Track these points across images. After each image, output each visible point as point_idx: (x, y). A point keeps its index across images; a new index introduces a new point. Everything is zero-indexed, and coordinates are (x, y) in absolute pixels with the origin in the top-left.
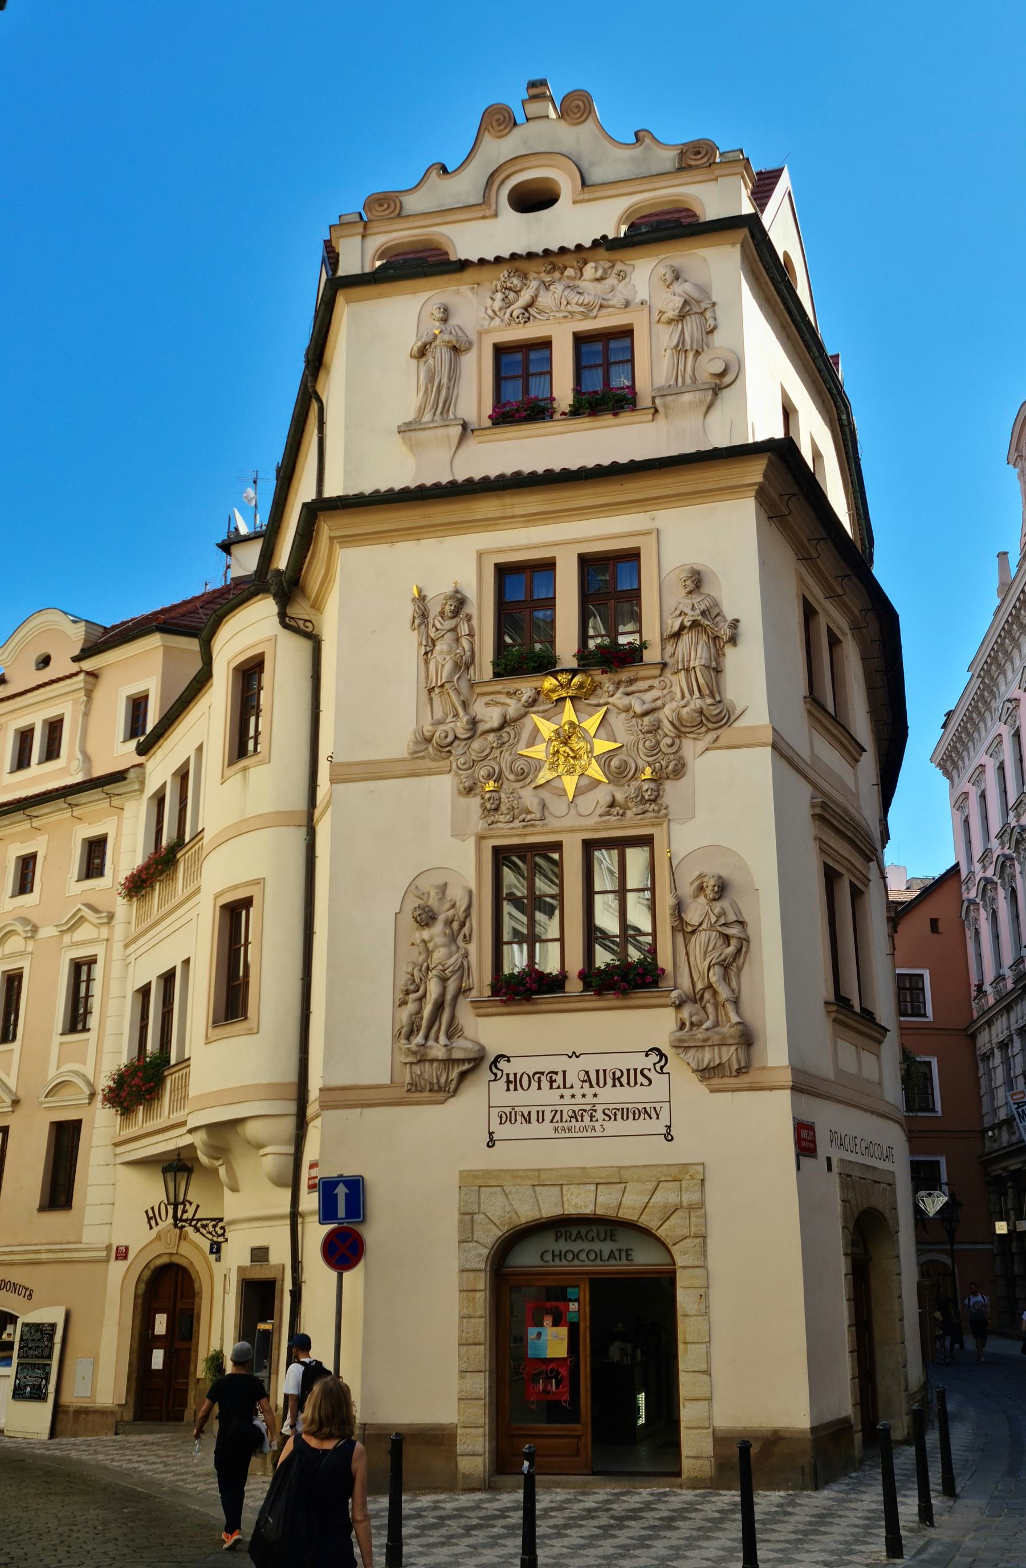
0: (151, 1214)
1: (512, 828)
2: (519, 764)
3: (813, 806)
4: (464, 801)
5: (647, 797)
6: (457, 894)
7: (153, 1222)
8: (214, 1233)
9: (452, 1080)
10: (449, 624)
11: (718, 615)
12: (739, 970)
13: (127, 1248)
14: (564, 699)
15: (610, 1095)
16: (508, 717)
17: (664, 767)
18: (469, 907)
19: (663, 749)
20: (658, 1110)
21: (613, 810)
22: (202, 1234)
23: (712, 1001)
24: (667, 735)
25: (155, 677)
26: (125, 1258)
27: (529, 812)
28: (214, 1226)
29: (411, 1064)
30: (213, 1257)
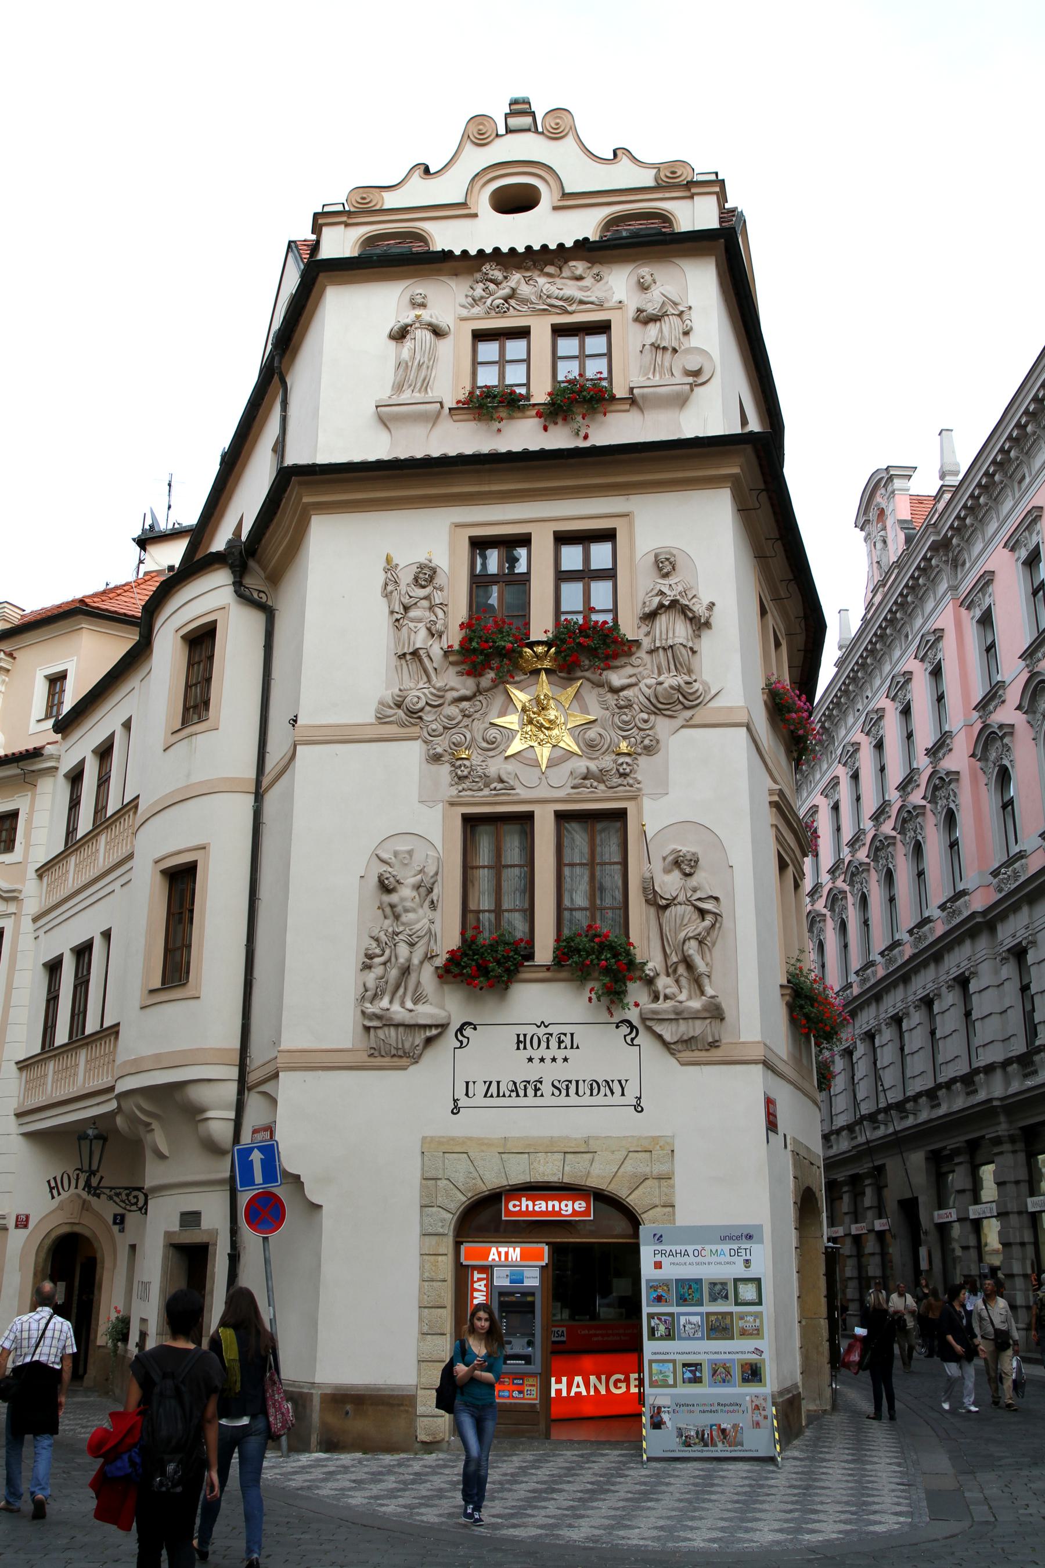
0: (53, 1184)
1: (483, 797)
2: (493, 733)
3: (771, 792)
4: (434, 768)
5: (621, 771)
6: (425, 858)
7: (55, 1192)
8: (127, 1202)
9: (417, 1046)
10: (422, 593)
11: (694, 596)
12: (714, 944)
13: (27, 1217)
14: (540, 670)
16: (481, 686)
17: (639, 741)
18: (437, 874)
19: (640, 725)
20: (623, 1083)
21: (586, 782)
22: (115, 1202)
23: (685, 974)
24: (642, 711)
25: (75, 658)
26: (26, 1226)
27: (502, 781)
28: (128, 1195)
29: (376, 1028)
30: (116, 1228)
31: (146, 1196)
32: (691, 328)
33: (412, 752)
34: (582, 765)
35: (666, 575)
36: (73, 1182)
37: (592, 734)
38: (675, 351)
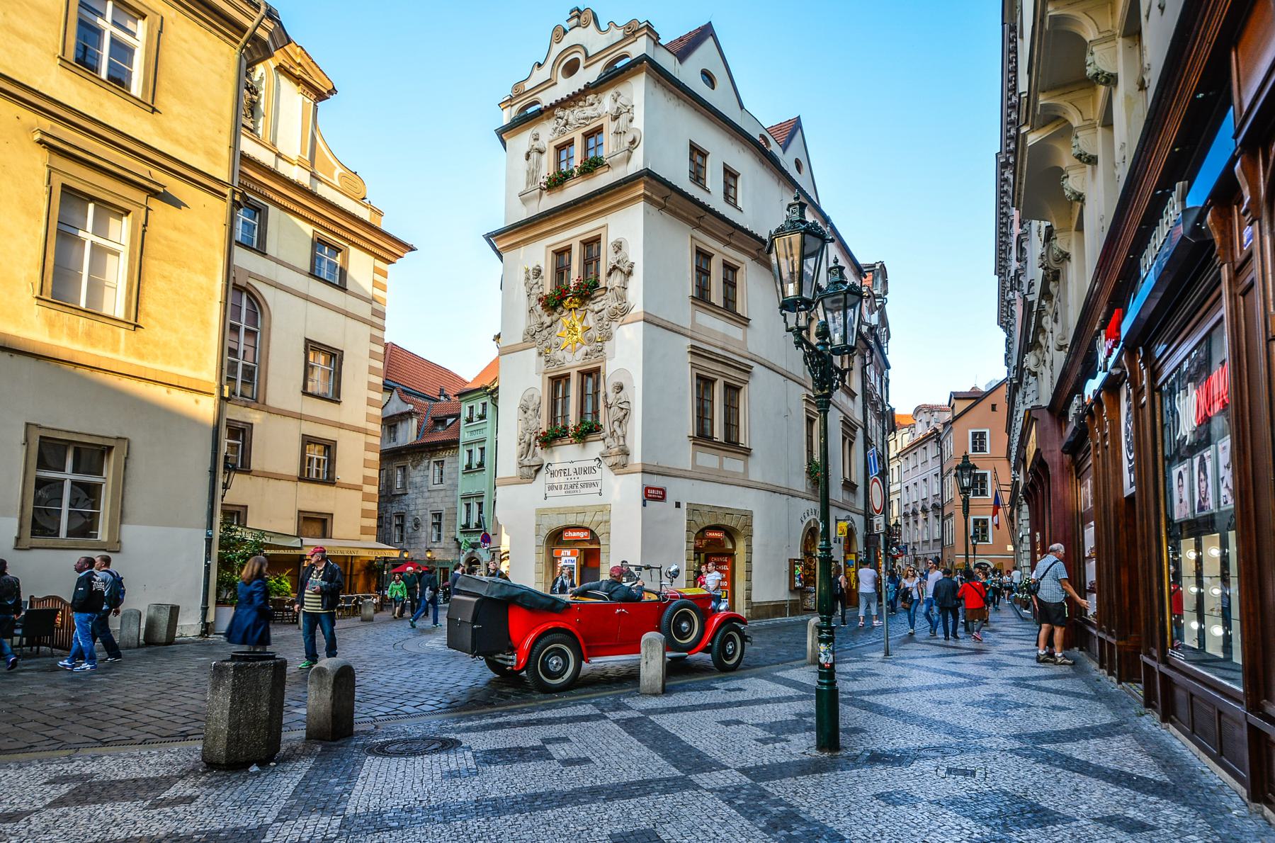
2: (558, 340)
4: (540, 358)
10: (535, 281)
15: (584, 478)
32: (633, 118)
33: (534, 351)
34: (586, 348)
35: (616, 252)
37: (589, 335)
38: (625, 132)
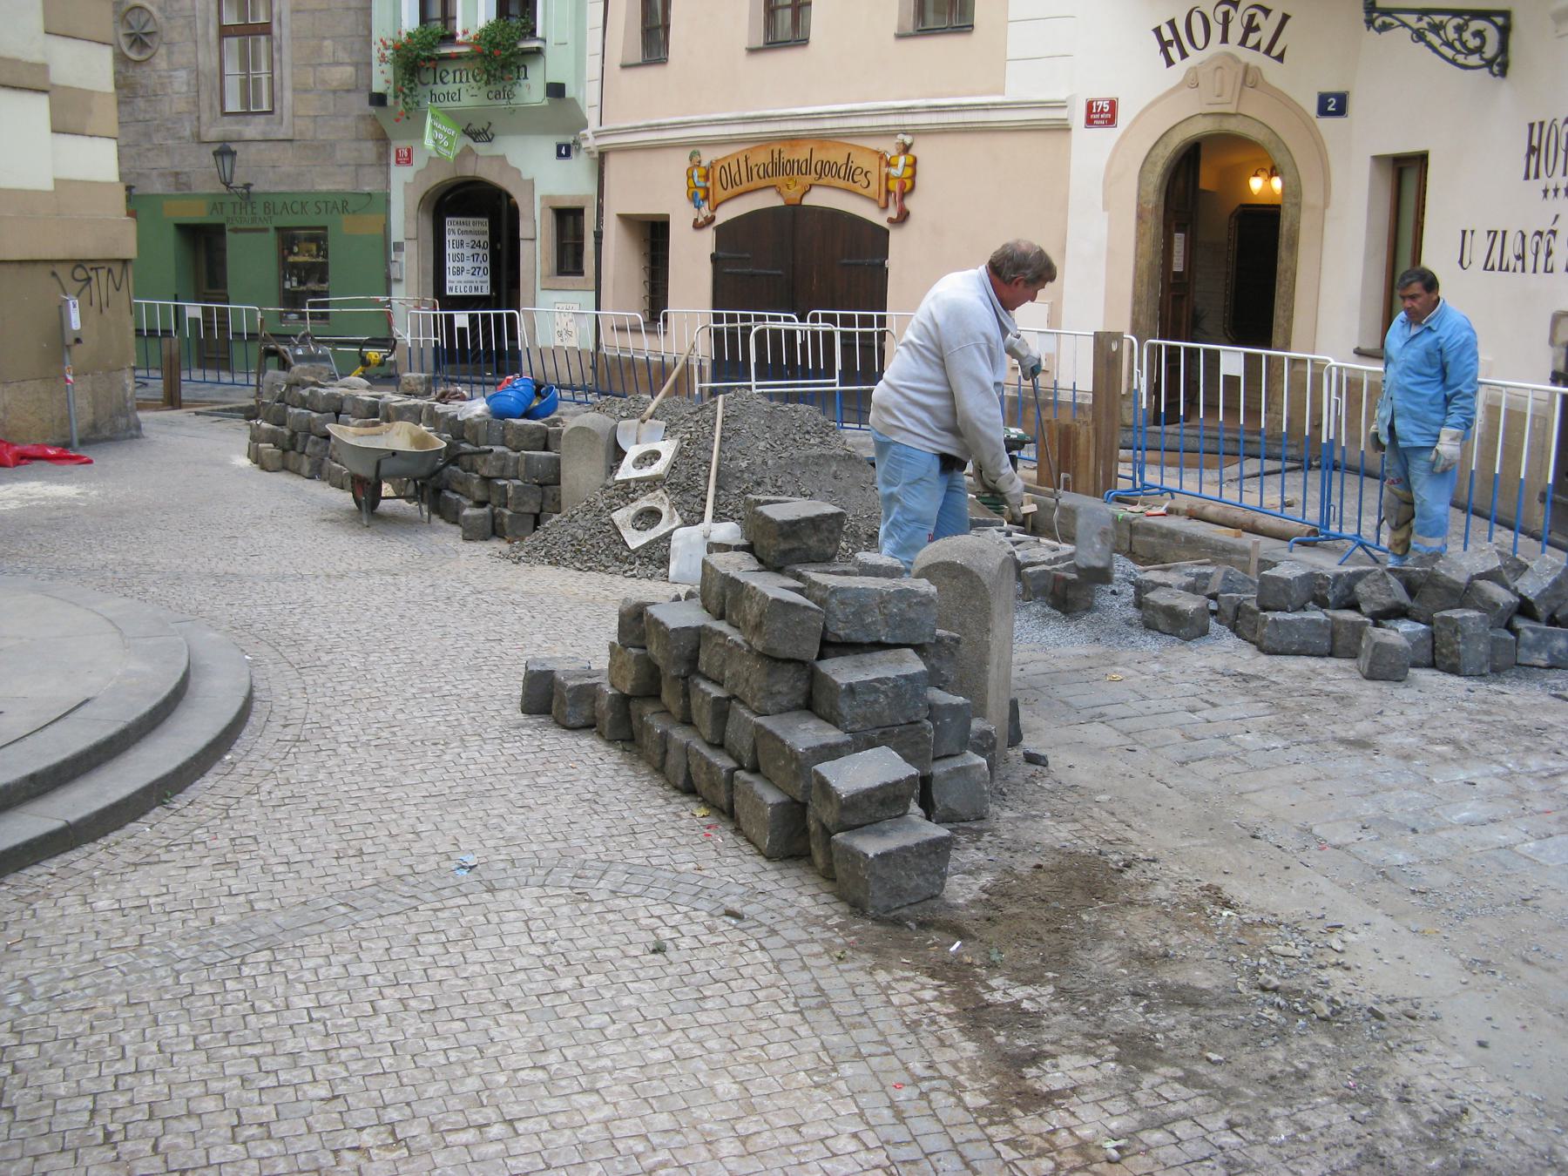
0: (1167, 35)
7: (1174, 52)
8: (1457, 44)
13: (1113, 104)
22: (1430, 45)
31: (1505, 31)
36: (1216, 31)
